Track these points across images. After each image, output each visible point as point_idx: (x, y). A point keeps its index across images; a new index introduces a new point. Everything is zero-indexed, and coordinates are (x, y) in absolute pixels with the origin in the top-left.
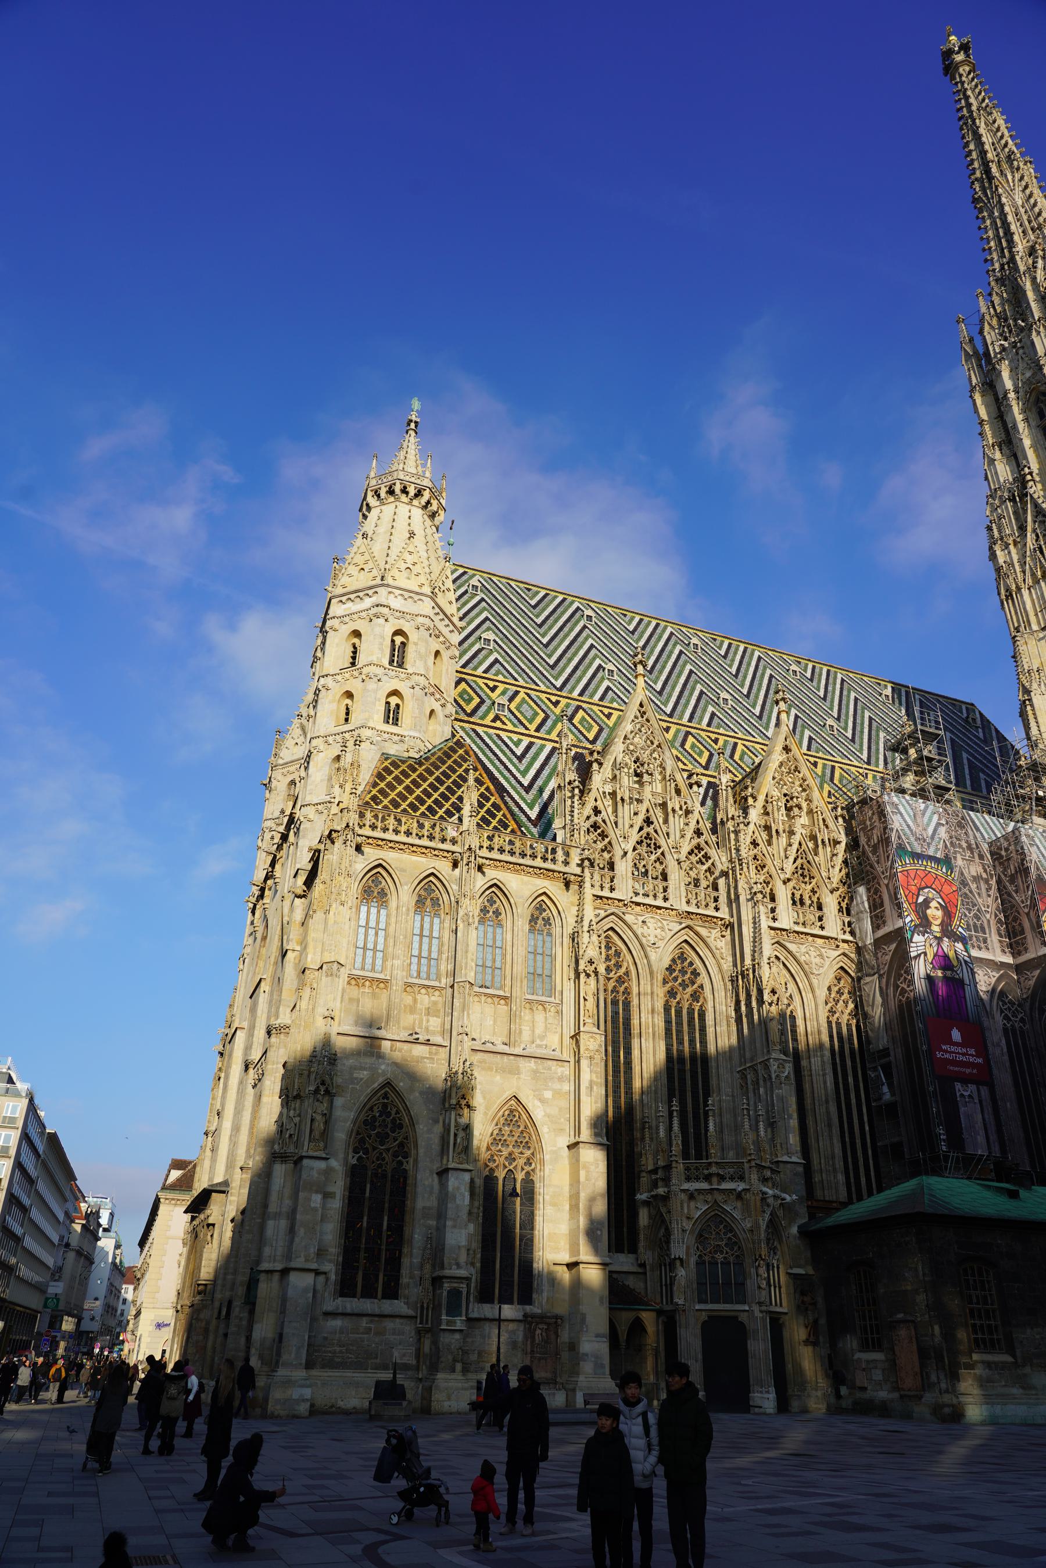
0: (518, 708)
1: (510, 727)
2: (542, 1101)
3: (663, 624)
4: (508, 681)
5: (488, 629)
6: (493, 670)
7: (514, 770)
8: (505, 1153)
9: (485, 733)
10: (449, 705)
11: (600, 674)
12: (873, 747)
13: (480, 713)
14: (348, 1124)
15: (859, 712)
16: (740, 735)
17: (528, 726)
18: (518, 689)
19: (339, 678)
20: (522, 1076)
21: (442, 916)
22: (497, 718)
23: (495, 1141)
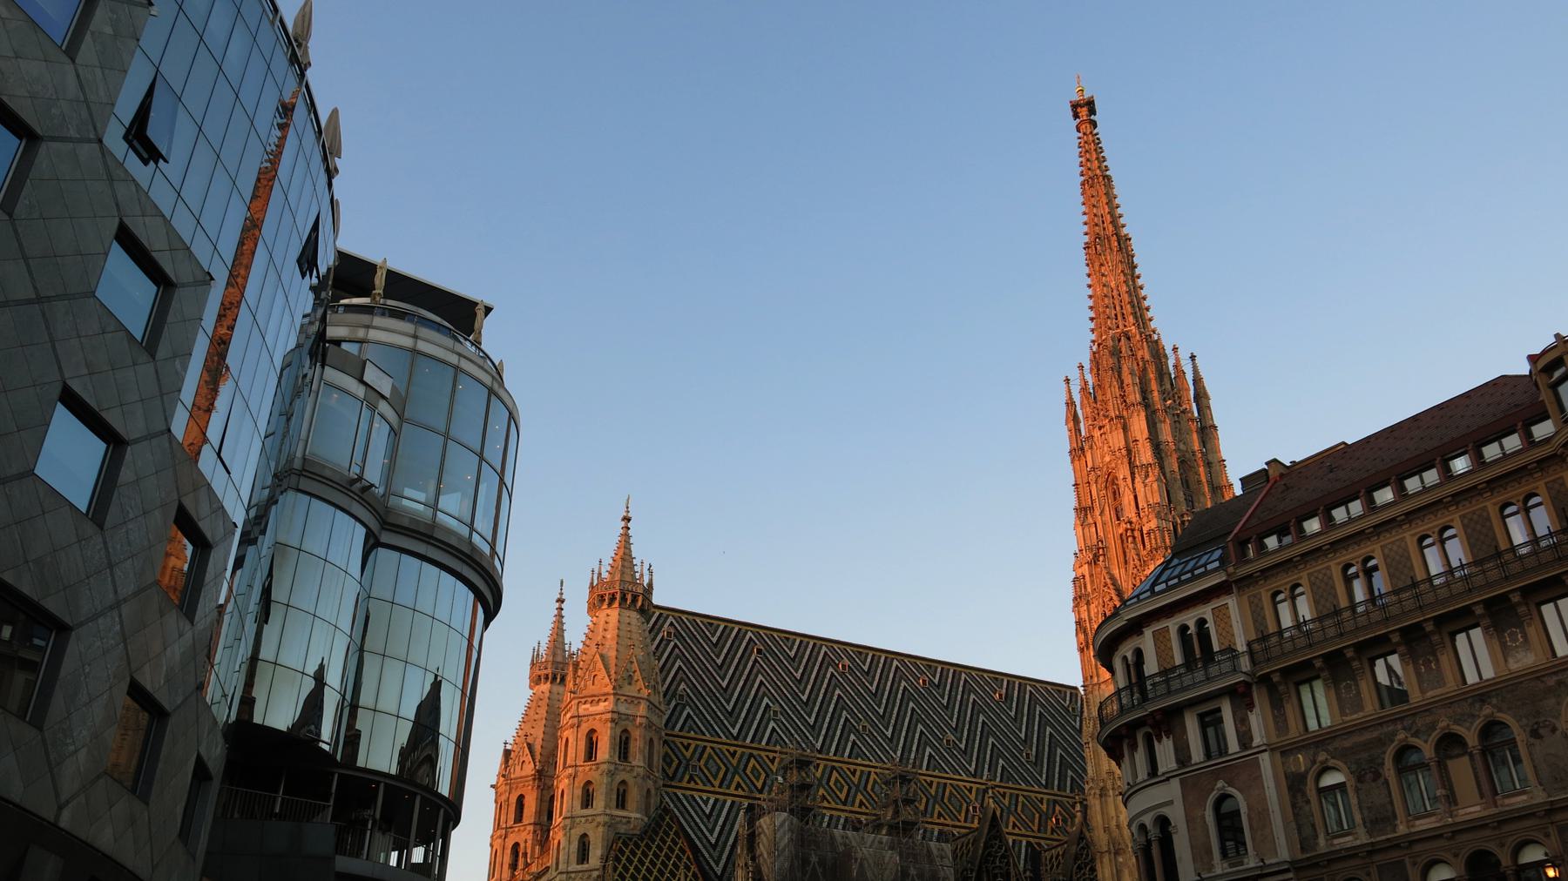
0: (705, 765)
1: (701, 787)
3: (819, 643)
5: (682, 680)
6: (686, 728)
7: (705, 830)
9: (684, 795)
10: (658, 780)
11: (767, 715)
12: (981, 756)
13: (679, 775)
15: (975, 717)
16: (874, 763)
18: (706, 744)
19: (581, 769)
22: (691, 779)
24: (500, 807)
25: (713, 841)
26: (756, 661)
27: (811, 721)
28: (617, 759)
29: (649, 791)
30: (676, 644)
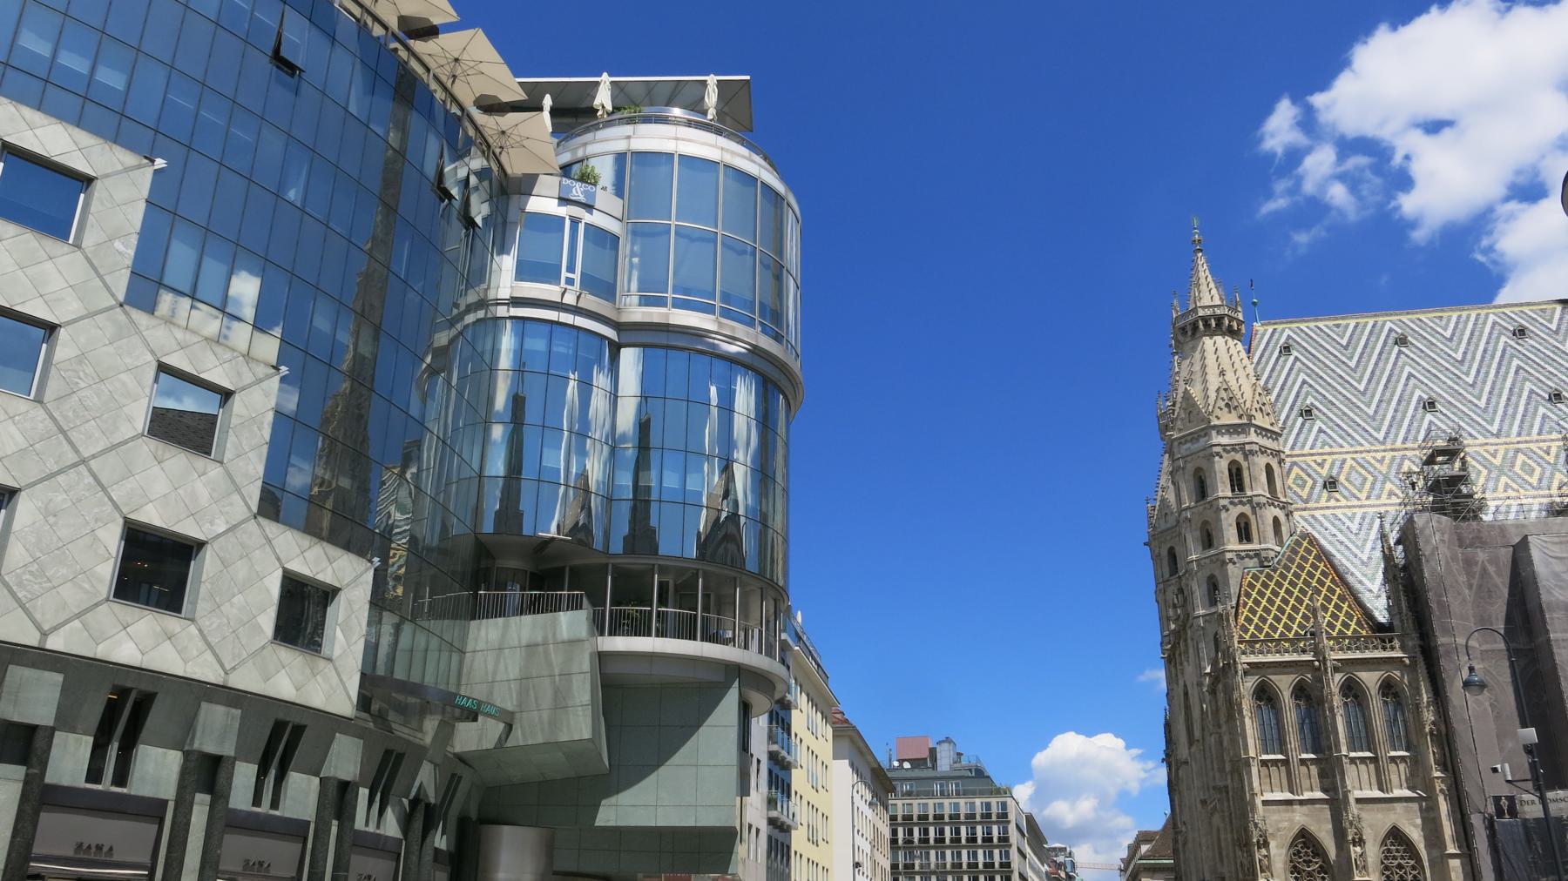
0: (1347, 480)
1: (1343, 502)
2: (1415, 826)
3: (1483, 312)
4: (1334, 450)
5: (1307, 394)
6: (1319, 444)
8: (1396, 863)
13: (1315, 496)
14: (1283, 858)
17: (1358, 494)
18: (1344, 456)
19: (1194, 510)
20: (1398, 812)
21: (1316, 706)
23: (1386, 858)
24: (1156, 558)
25: (1365, 558)
26: (1400, 352)
27: (1482, 404)
28: (1229, 494)
29: (1276, 520)
30: (1297, 359)
